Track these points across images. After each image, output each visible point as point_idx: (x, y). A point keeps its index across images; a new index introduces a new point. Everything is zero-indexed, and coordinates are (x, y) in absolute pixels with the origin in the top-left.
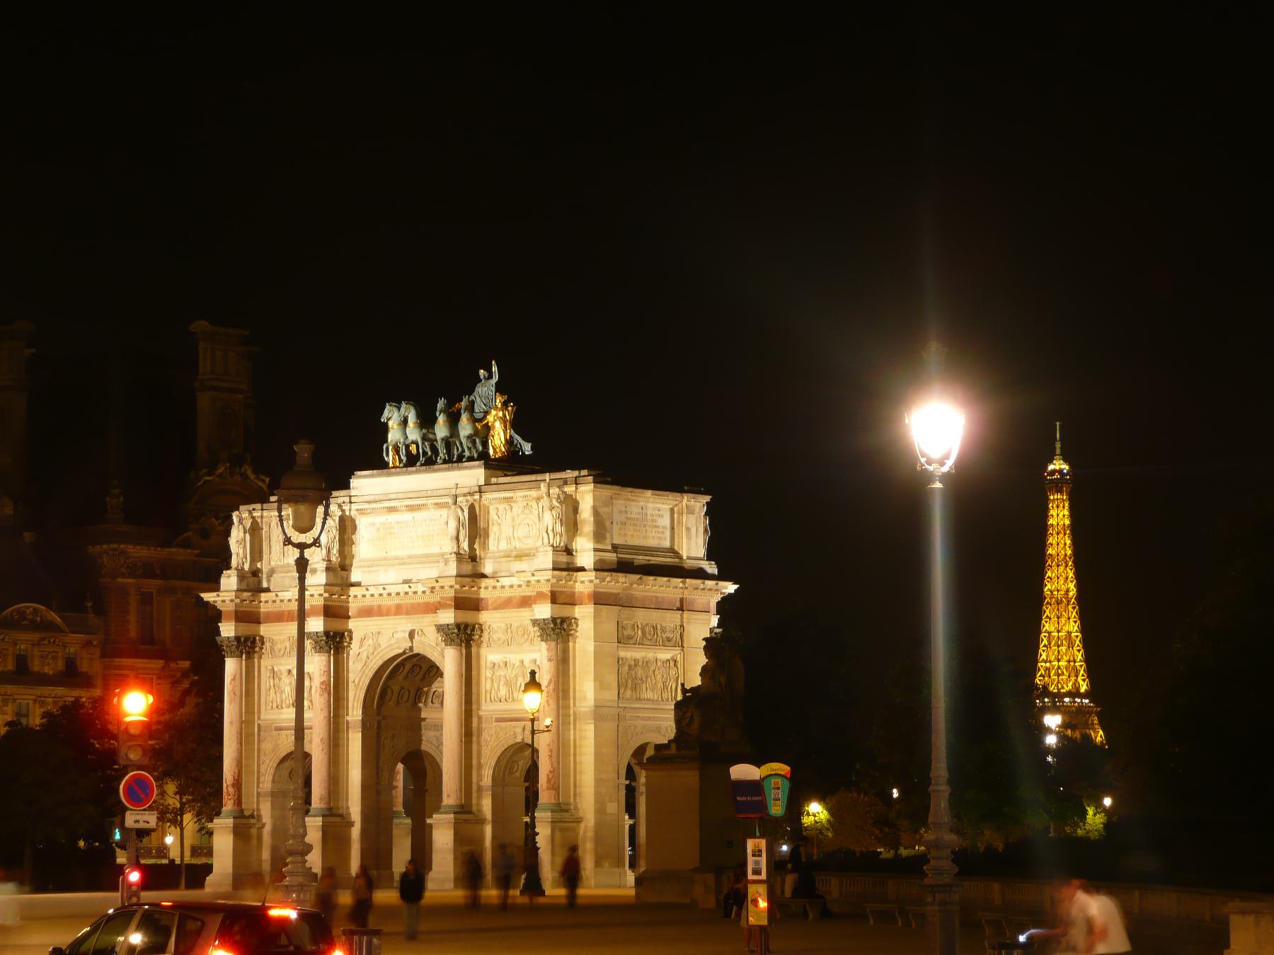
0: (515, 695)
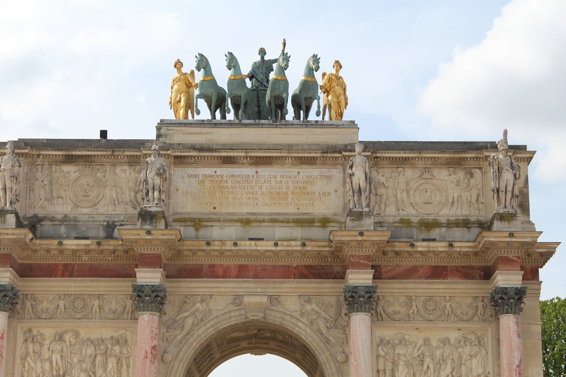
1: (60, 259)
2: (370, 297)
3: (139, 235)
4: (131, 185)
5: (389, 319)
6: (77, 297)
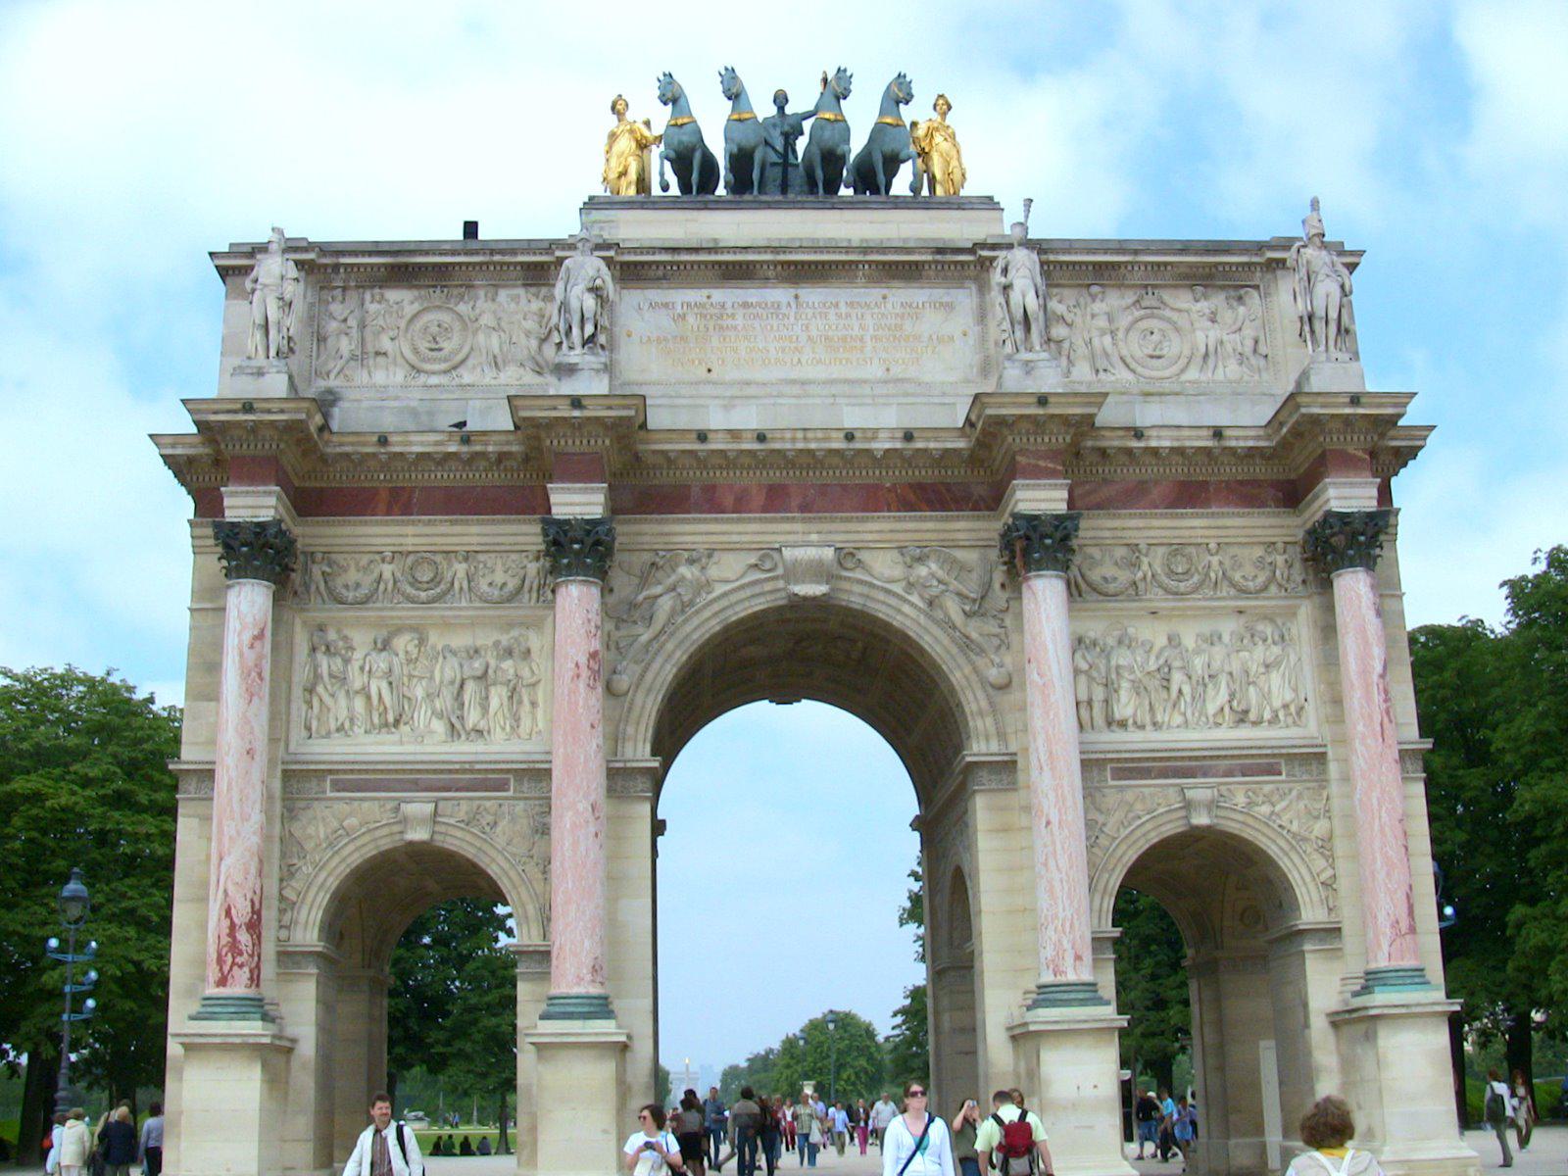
0: (1159, 718)
1: (382, 477)
2: (1066, 538)
3: (555, 409)
4: (530, 324)
5: (1095, 596)
6: (422, 558)
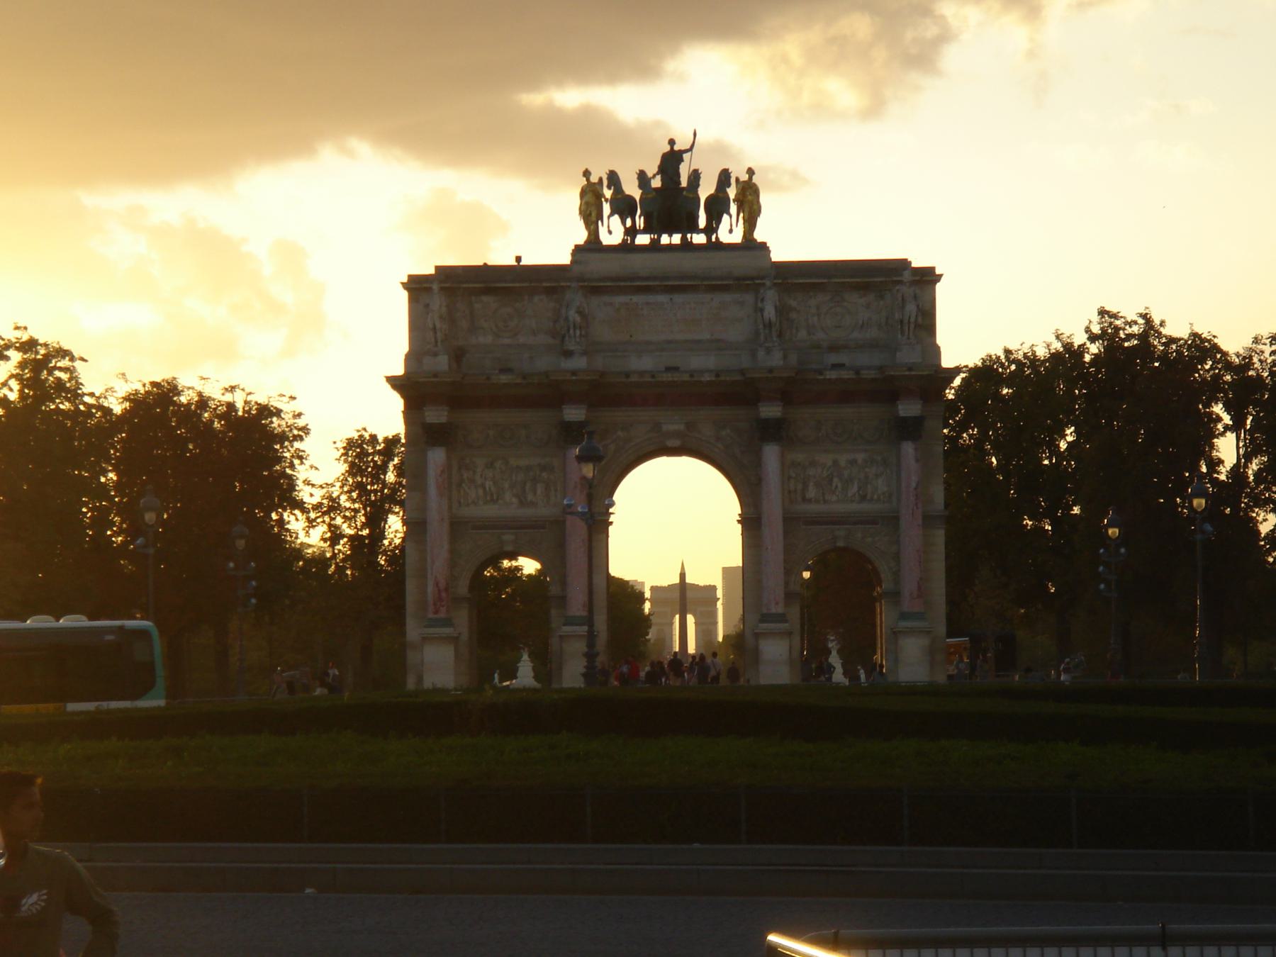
0: (826, 498)
